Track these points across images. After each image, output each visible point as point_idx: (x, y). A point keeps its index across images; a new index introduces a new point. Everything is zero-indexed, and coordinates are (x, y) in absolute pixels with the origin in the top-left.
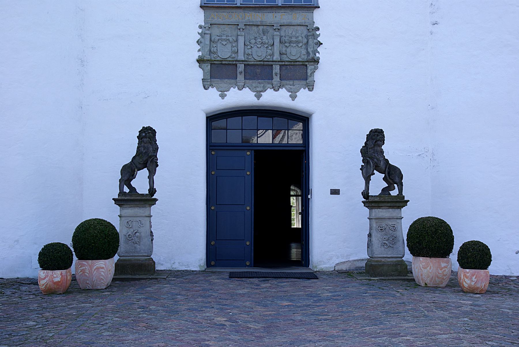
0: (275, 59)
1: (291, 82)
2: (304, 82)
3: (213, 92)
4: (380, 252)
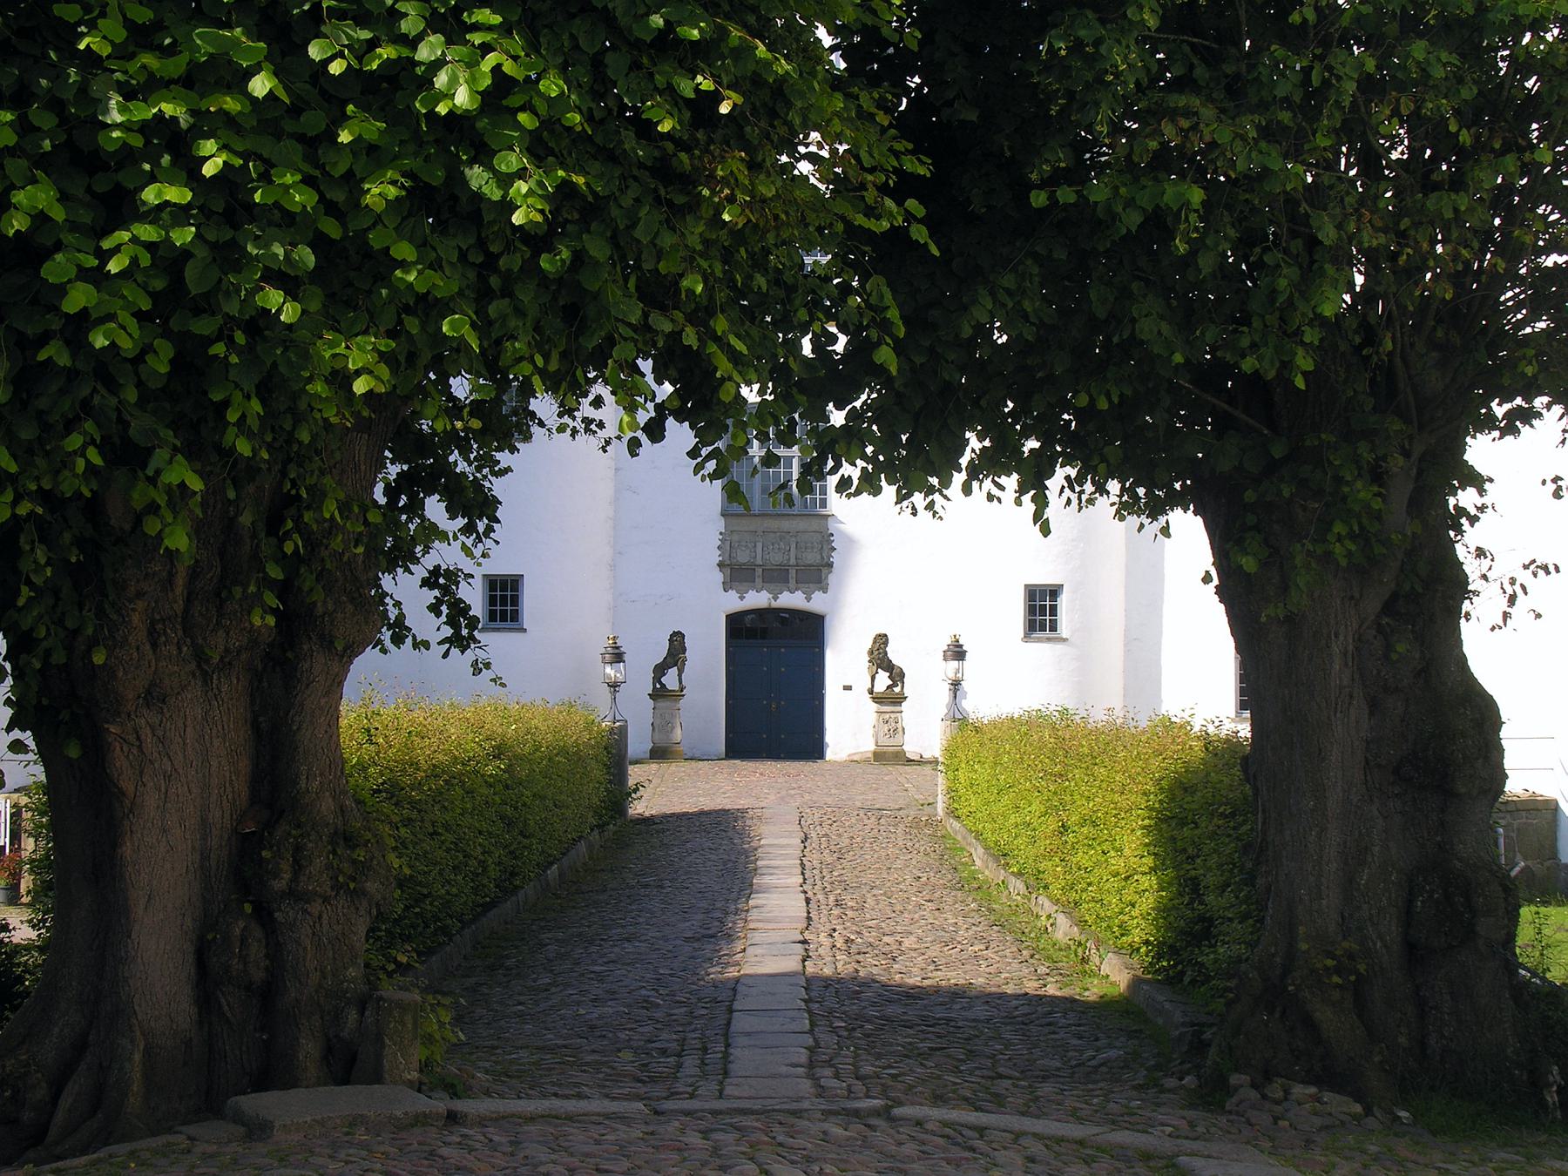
0: (791, 563)
1: (807, 585)
2: (818, 585)
3: (733, 594)
4: (885, 741)
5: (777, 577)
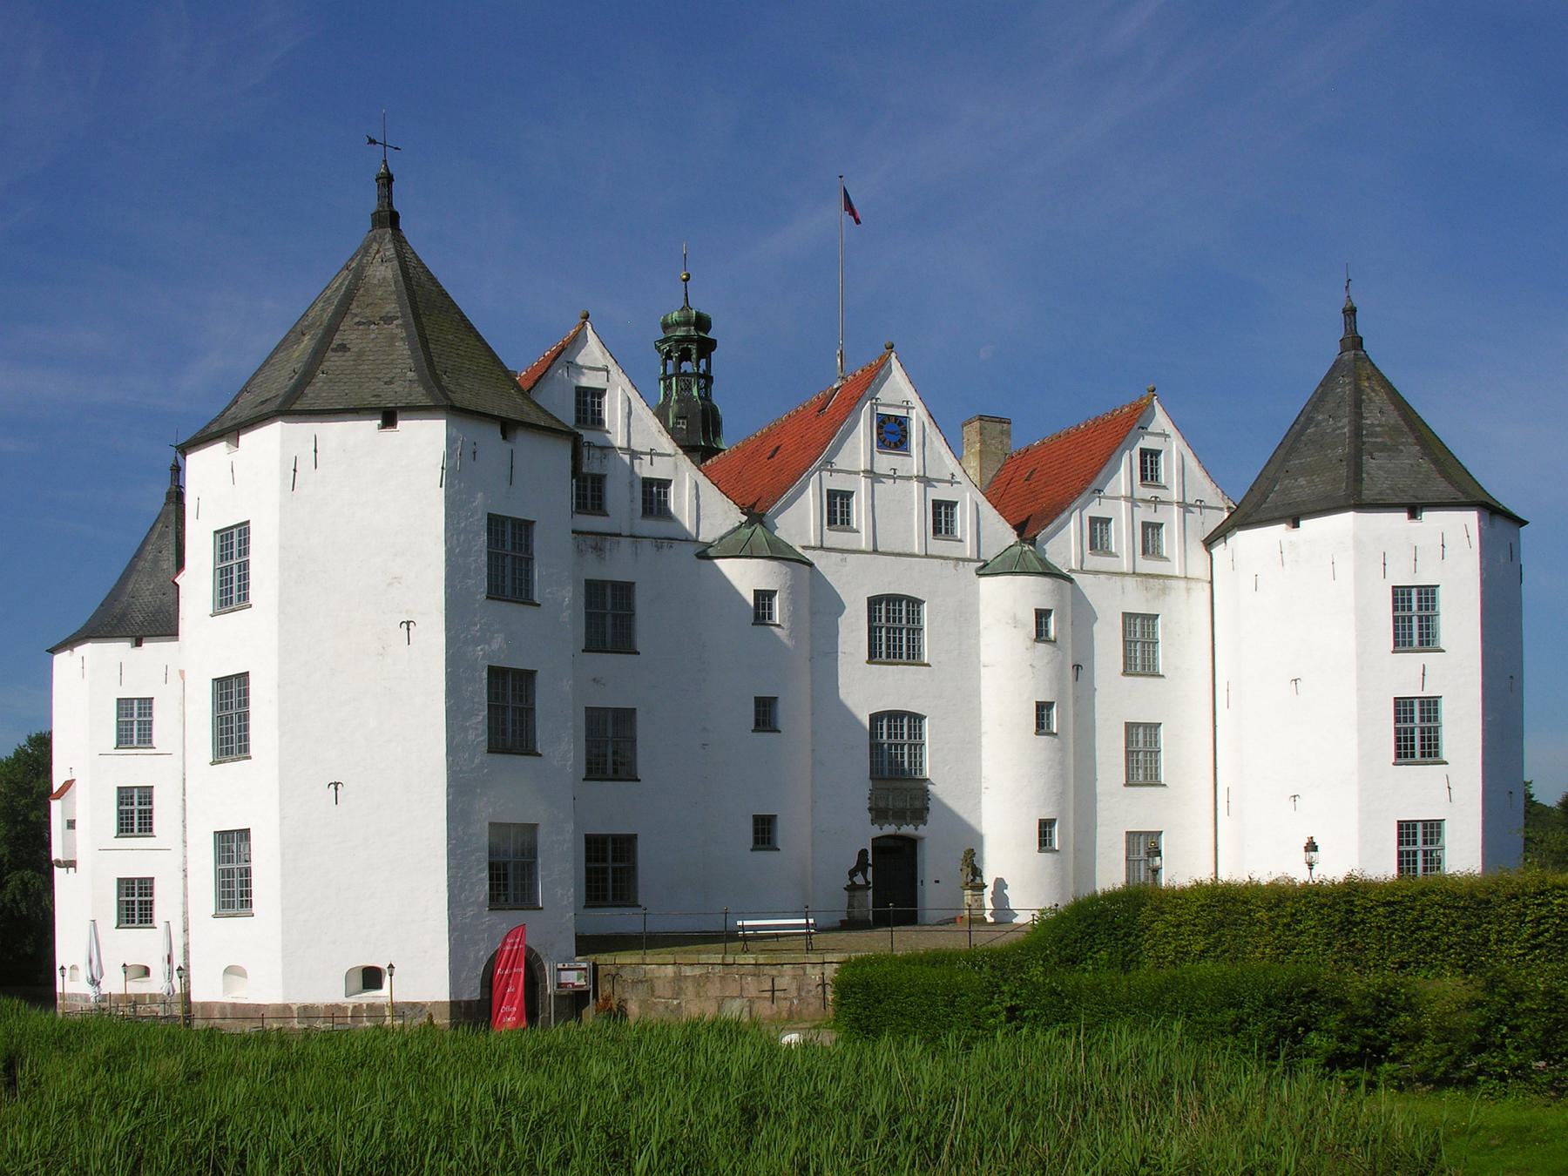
5: (900, 816)
